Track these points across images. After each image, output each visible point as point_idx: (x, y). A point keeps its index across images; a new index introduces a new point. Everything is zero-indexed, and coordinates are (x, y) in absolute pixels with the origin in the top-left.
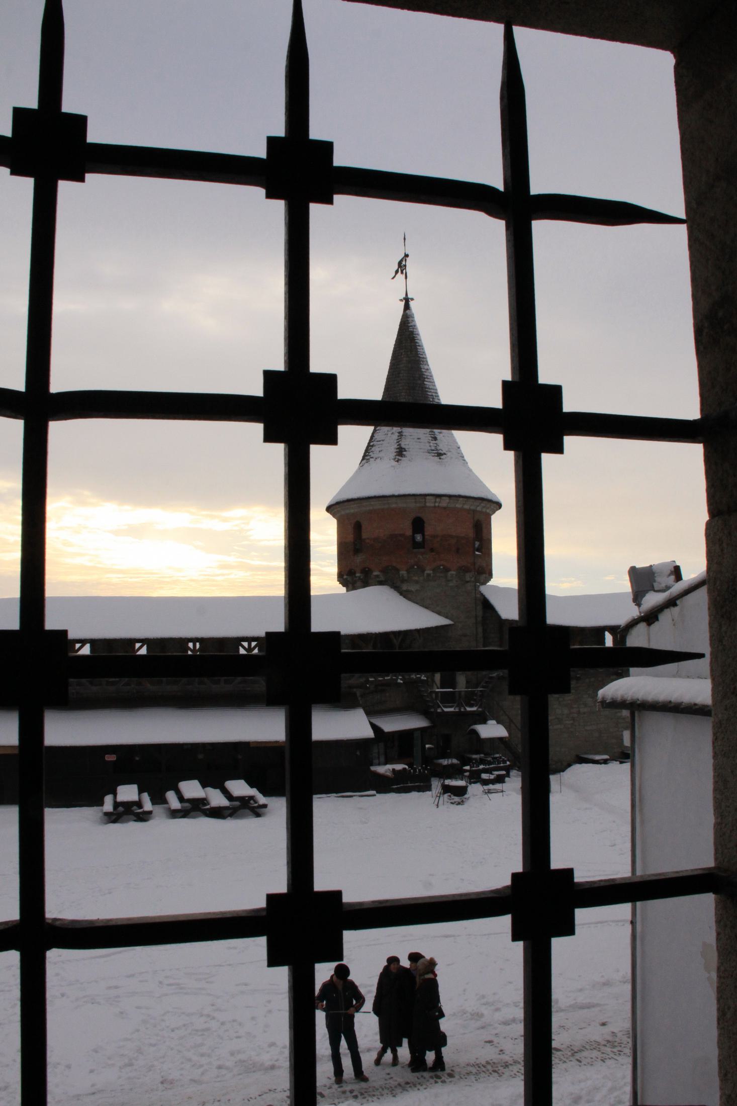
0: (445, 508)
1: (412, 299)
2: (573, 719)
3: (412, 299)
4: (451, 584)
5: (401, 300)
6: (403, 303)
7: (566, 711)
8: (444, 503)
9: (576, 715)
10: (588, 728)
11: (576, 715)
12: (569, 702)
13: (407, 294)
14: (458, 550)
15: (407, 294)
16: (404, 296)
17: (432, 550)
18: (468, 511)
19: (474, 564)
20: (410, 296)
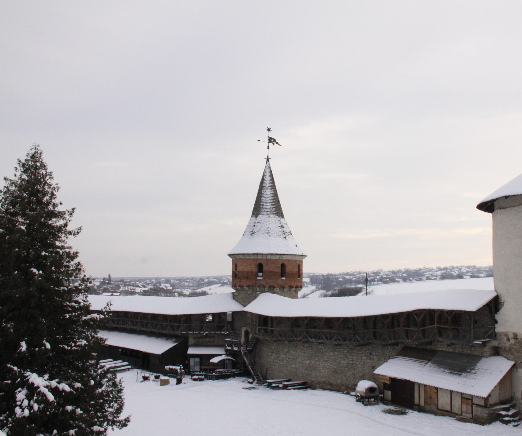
0: (243, 259)
1: (270, 159)
2: (287, 361)
3: (270, 159)
4: (249, 293)
5: (265, 158)
6: (266, 160)
7: (284, 357)
8: (241, 257)
9: (288, 359)
10: (292, 366)
11: (288, 359)
12: (286, 352)
13: (268, 157)
14: (247, 278)
15: (268, 157)
16: (267, 157)
17: (238, 278)
18: (254, 260)
19: (256, 283)
20: (269, 157)
